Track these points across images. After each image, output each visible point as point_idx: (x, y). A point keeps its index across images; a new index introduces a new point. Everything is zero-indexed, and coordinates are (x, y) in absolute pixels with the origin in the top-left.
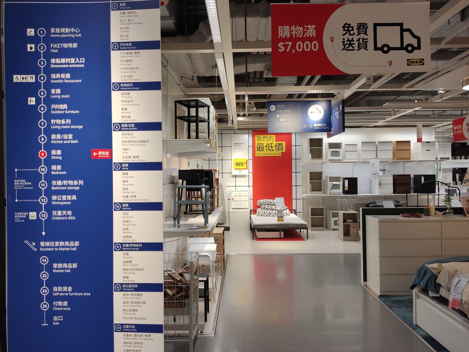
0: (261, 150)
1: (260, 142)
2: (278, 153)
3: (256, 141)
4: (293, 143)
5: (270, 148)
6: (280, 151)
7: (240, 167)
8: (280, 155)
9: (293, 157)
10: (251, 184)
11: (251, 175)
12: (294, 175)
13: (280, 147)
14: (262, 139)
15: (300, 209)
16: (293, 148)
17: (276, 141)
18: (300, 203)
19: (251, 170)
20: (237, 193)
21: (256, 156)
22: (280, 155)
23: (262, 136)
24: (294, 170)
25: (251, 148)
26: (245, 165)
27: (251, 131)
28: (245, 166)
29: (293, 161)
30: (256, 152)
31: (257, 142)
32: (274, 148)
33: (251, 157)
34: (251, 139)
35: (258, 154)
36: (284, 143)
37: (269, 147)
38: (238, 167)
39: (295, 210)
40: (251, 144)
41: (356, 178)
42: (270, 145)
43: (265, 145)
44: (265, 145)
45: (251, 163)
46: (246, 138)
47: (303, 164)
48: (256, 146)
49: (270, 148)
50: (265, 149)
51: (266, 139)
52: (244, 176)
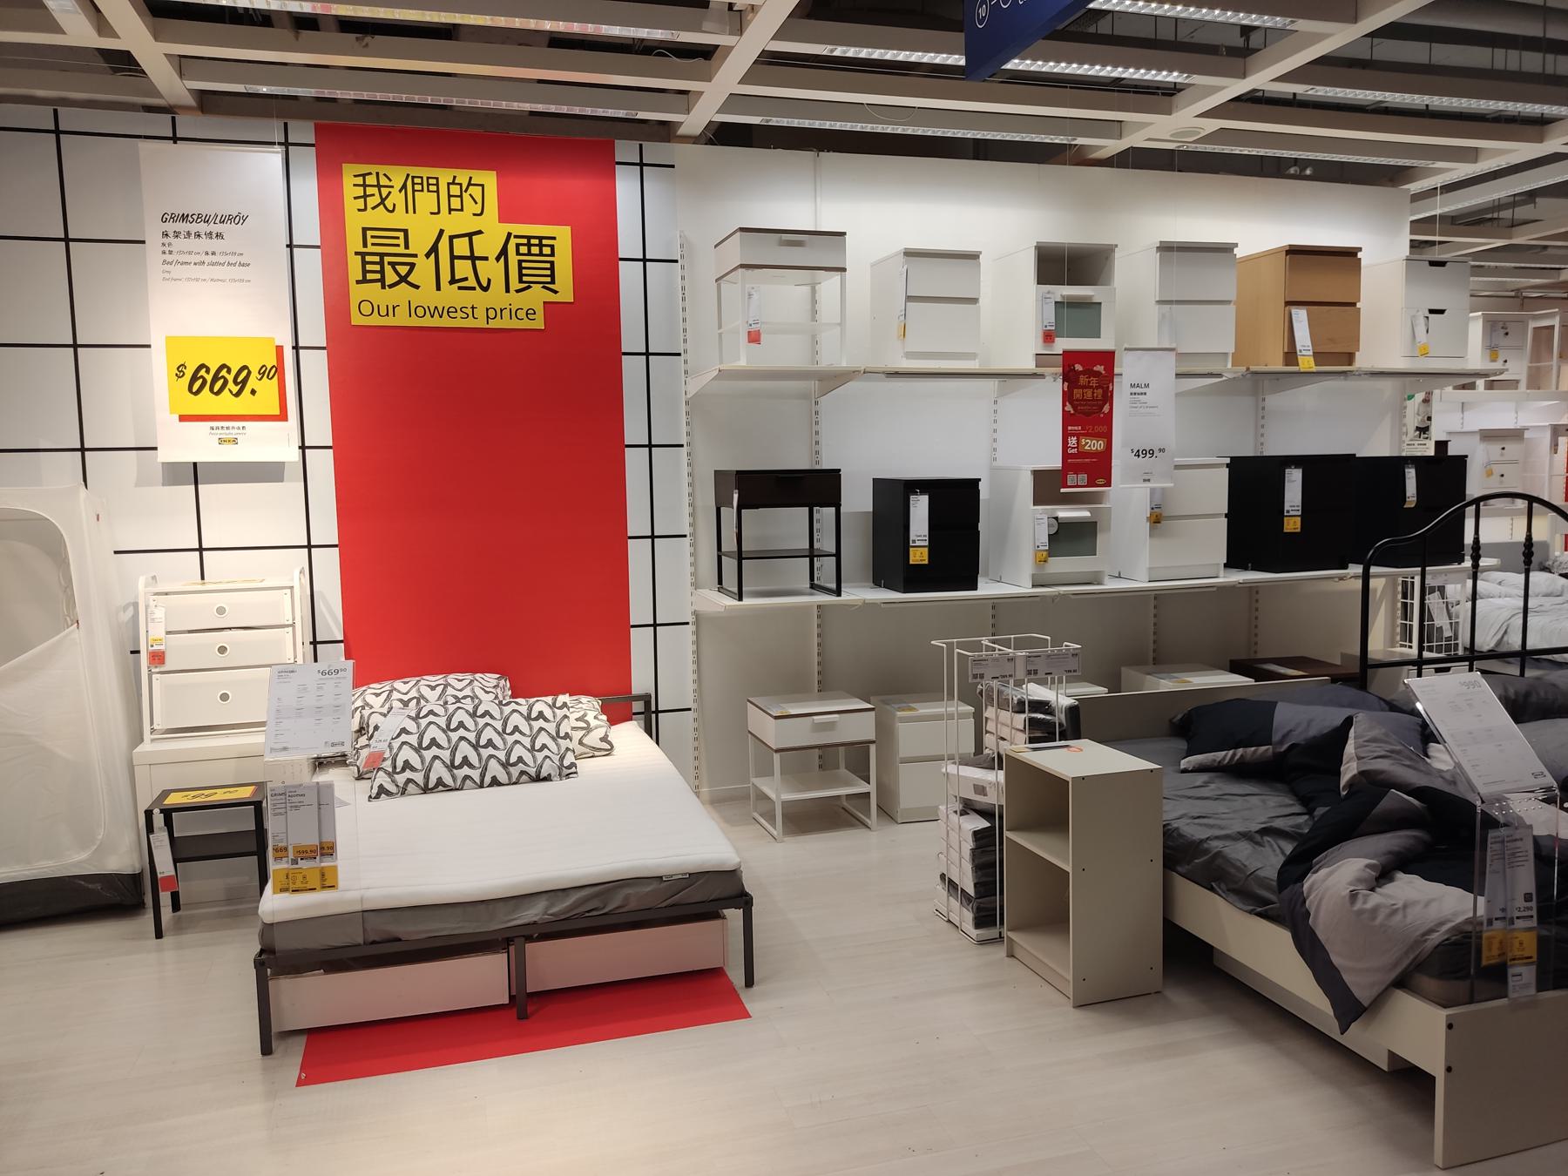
0: (391, 277)
1: (378, 218)
2: (522, 308)
3: (351, 205)
4: (628, 244)
5: (463, 268)
6: (537, 297)
7: (226, 403)
8: (539, 323)
9: (631, 338)
10: (327, 528)
11: (323, 466)
12: (635, 461)
13: (536, 268)
14: (396, 198)
15: (677, 688)
16: (629, 275)
17: (502, 219)
18: (679, 646)
19: (321, 428)
20: (202, 608)
21: (357, 319)
22: (539, 323)
23: (397, 175)
24: (634, 431)
25: (311, 265)
26: (268, 388)
27: (303, 131)
28: (265, 395)
29: (632, 369)
30: (357, 293)
31: (354, 221)
32: (491, 270)
33: (314, 330)
34: (307, 189)
35: (377, 305)
36: (562, 236)
37: (457, 255)
38: (206, 402)
39: (646, 699)
40: (309, 228)
41: (972, 485)
42: (461, 247)
43: (420, 244)
44: (420, 244)
45: (316, 368)
46: (261, 180)
47: (694, 386)
48: (354, 243)
49: (463, 268)
50: (424, 271)
51: (426, 200)
52: (268, 472)
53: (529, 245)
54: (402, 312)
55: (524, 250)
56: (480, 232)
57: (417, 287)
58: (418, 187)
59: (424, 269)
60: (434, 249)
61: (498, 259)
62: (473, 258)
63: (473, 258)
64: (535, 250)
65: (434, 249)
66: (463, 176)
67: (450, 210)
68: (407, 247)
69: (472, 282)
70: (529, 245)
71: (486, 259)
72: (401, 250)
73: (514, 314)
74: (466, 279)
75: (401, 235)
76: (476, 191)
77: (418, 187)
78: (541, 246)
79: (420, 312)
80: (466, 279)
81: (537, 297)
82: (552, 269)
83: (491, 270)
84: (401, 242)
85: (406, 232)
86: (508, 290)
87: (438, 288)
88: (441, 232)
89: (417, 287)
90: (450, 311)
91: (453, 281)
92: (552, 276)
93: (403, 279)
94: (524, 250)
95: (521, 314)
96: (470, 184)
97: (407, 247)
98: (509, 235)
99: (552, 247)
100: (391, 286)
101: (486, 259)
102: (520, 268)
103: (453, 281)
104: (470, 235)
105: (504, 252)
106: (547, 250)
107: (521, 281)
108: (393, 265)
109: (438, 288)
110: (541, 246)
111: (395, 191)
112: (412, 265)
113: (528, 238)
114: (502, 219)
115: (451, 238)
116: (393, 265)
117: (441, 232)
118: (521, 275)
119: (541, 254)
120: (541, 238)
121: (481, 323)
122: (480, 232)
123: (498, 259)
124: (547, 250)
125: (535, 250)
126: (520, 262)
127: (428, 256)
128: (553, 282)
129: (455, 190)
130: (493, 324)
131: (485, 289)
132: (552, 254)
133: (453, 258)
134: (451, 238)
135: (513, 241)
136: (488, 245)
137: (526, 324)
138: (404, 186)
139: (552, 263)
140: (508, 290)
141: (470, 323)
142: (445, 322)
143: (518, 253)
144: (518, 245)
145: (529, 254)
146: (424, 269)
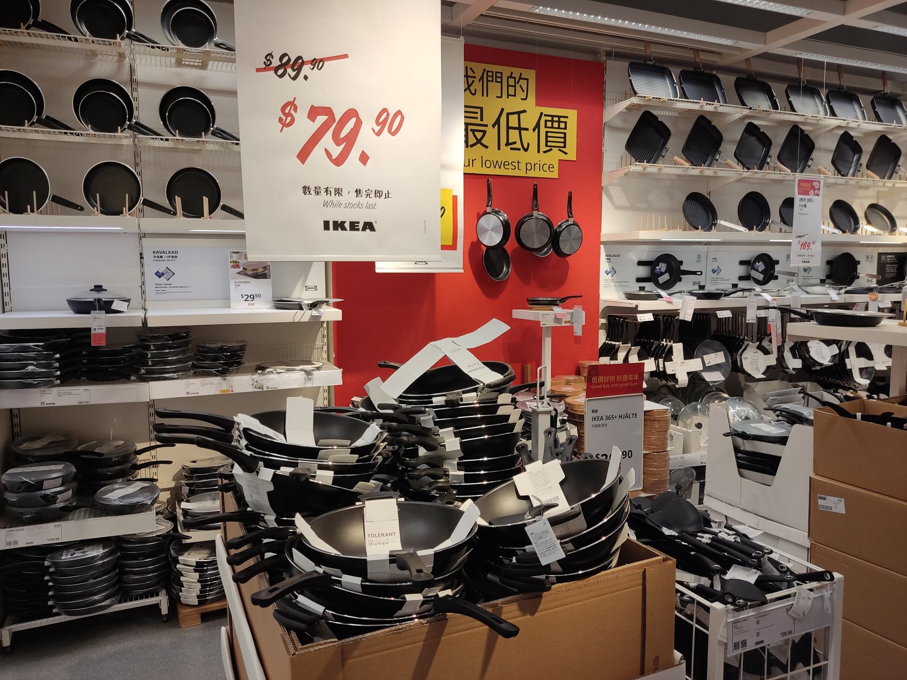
5: (514, 135)
8: (555, 175)
22: (555, 175)
32: (530, 137)
44: (489, 119)
51: (494, 88)
53: (552, 121)
54: (478, 163)
55: (549, 124)
56: (524, 111)
57: (487, 147)
58: (490, 79)
59: (492, 133)
60: (497, 122)
61: (534, 130)
62: (520, 129)
63: (520, 129)
64: (556, 125)
65: (497, 122)
66: (517, 72)
67: (508, 95)
68: (482, 120)
69: (518, 145)
70: (552, 121)
71: (527, 129)
72: (478, 121)
73: (541, 168)
74: (515, 143)
75: (479, 111)
76: (523, 83)
77: (490, 79)
78: (559, 122)
79: (488, 164)
80: (515, 143)
81: (555, 156)
82: (565, 138)
83: (530, 137)
84: (478, 116)
85: (481, 109)
86: (539, 152)
87: (499, 149)
88: (502, 110)
89: (487, 147)
90: (505, 164)
91: (508, 144)
92: (565, 142)
93: (479, 141)
94: (549, 124)
95: (546, 168)
96: (520, 78)
97: (482, 120)
98: (542, 114)
99: (566, 123)
100: (472, 146)
101: (527, 129)
102: (547, 137)
103: (508, 144)
104: (519, 113)
105: (538, 125)
106: (562, 125)
107: (547, 146)
108: (473, 131)
109: (499, 149)
110: (559, 122)
111: (476, 80)
112: (484, 132)
113: (553, 116)
114: (538, 104)
115: (508, 114)
116: (473, 131)
117: (502, 110)
118: (547, 141)
119: (559, 128)
120: (559, 117)
121: (522, 173)
122: (524, 111)
123: (534, 130)
124: (562, 125)
125: (556, 125)
126: (547, 132)
127: (494, 126)
128: (565, 147)
129: (512, 82)
130: (531, 174)
131: (526, 150)
132: (565, 128)
133: (508, 128)
134: (508, 114)
135: (544, 118)
136: (528, 121)
137: (548, 175)
138: (482, 78)
139: (565, 134)
140: (539, 152)
141: (516, 173)
142: (502, 172)
143: (546, 127)
144: (546, 121)
145: (552, 127)
146: (492, 133)
